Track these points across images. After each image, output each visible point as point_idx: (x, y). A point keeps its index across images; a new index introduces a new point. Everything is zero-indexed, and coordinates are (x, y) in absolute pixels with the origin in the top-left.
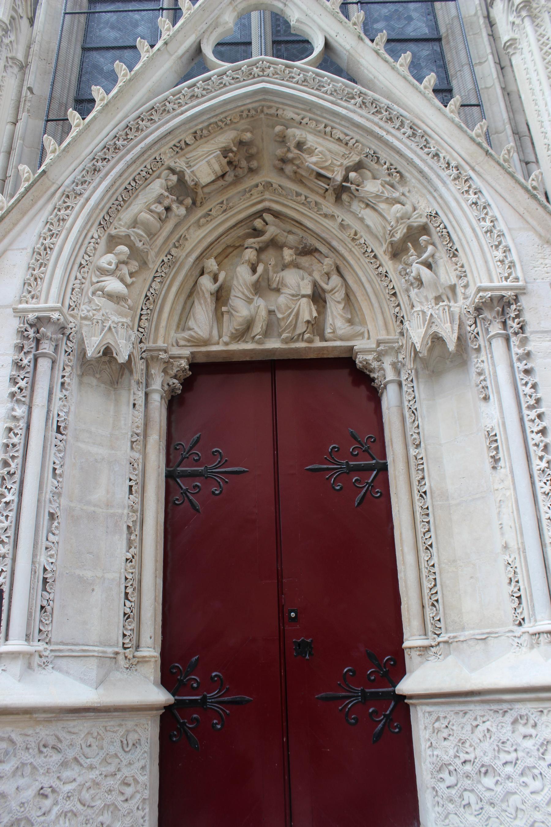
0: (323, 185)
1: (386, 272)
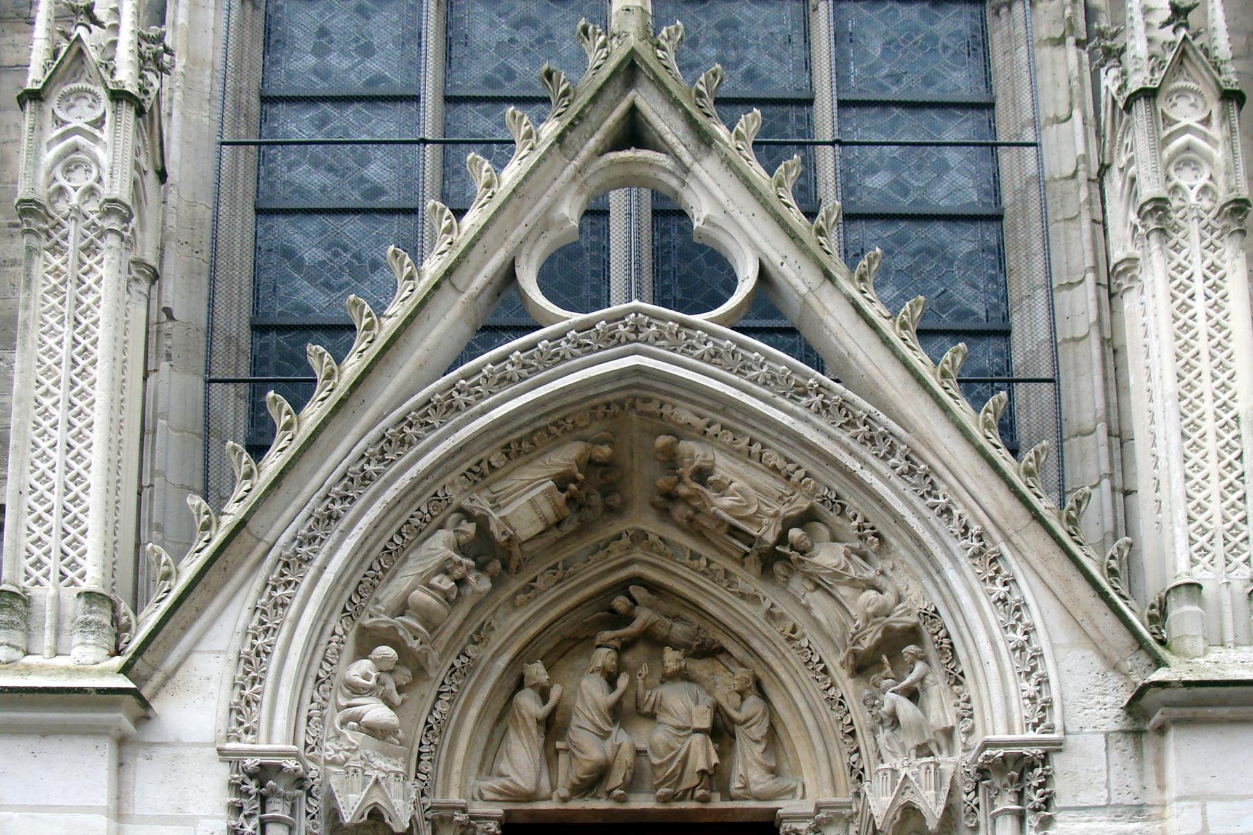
0: (740, 545)
1: (842, 697)
